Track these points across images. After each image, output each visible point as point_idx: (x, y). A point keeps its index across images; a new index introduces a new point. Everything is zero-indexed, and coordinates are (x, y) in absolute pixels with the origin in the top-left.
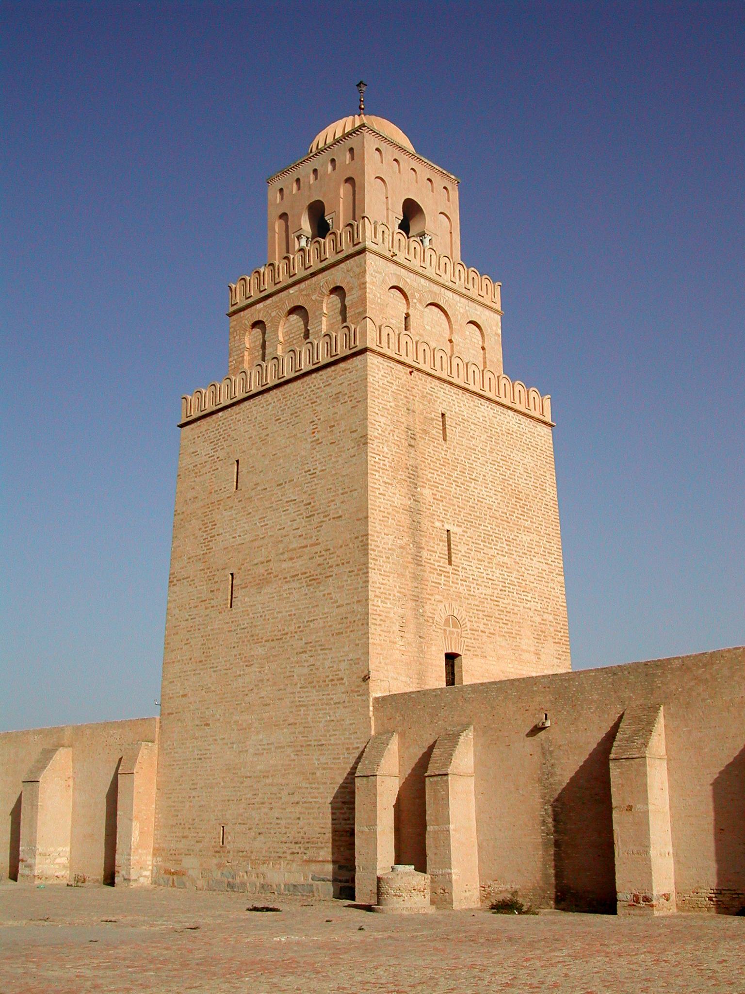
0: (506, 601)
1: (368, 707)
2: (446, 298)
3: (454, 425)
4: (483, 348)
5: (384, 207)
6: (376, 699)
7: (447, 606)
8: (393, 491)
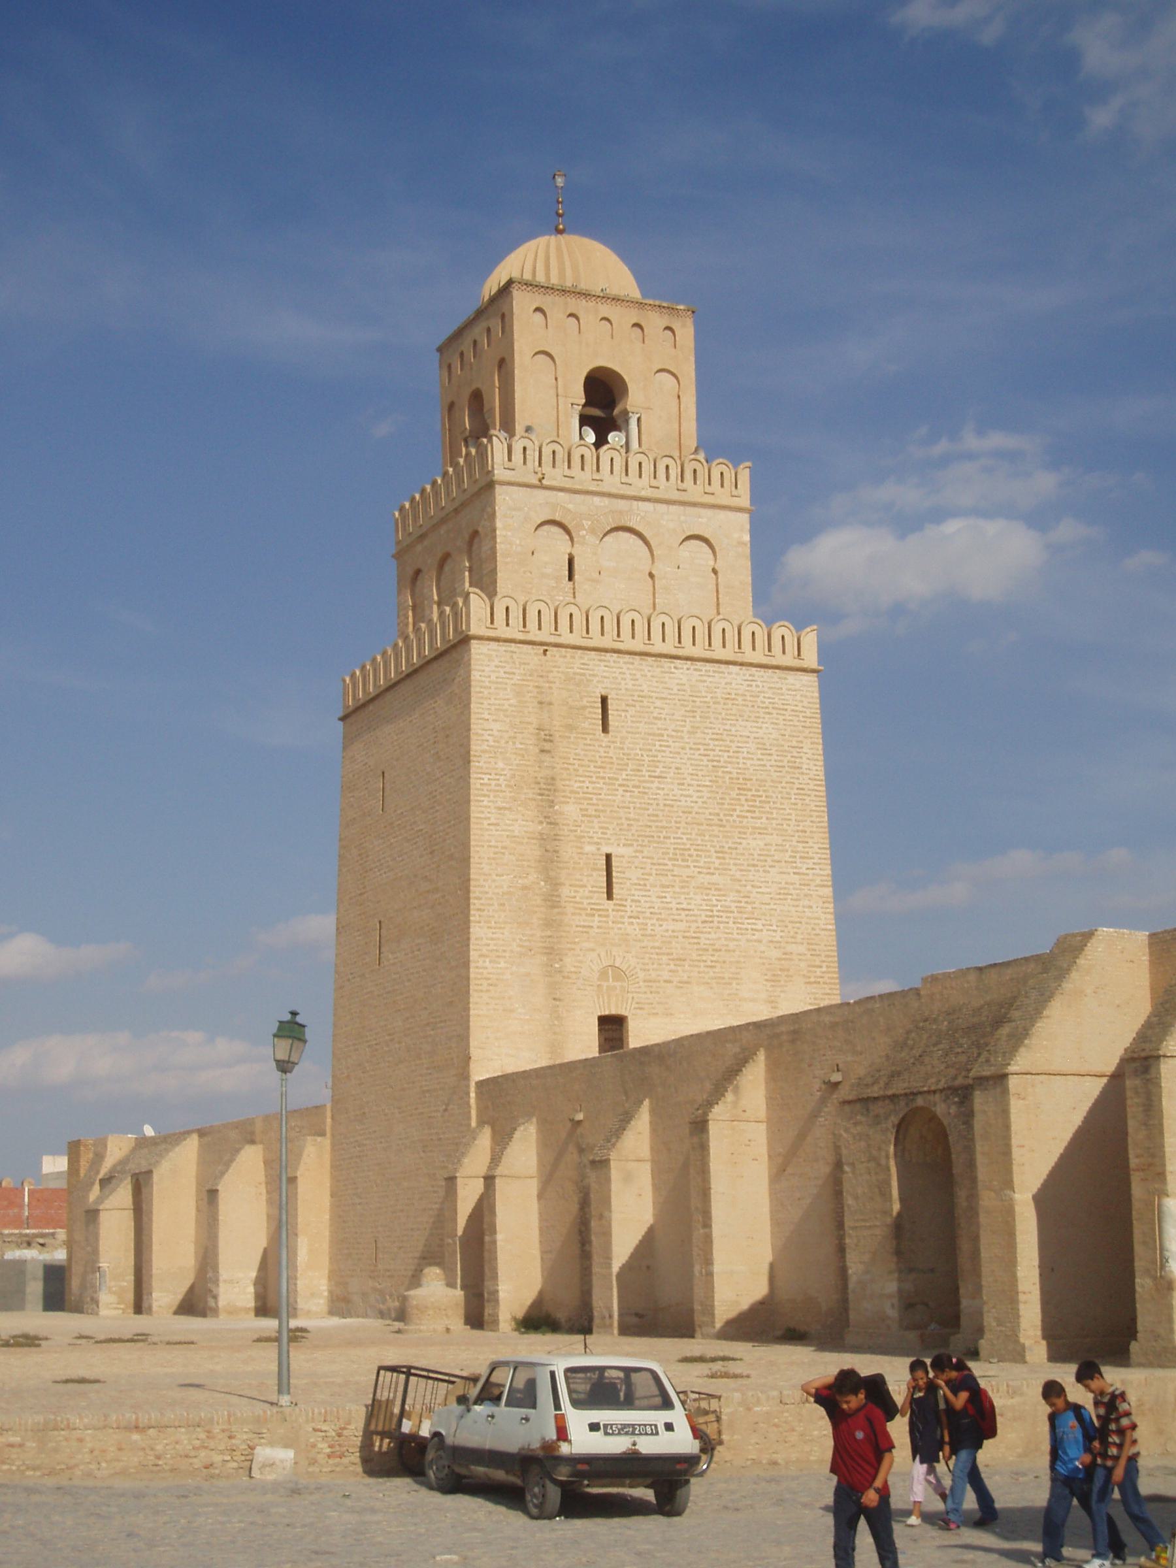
0: (713, 936)
1: (468, 1094)
2: (639, 515)
3: (624, 707)
4: (715, 571)
5: (553, 392)
6: (480, 1084)
7: (603, 954)
8: (511, 817)
